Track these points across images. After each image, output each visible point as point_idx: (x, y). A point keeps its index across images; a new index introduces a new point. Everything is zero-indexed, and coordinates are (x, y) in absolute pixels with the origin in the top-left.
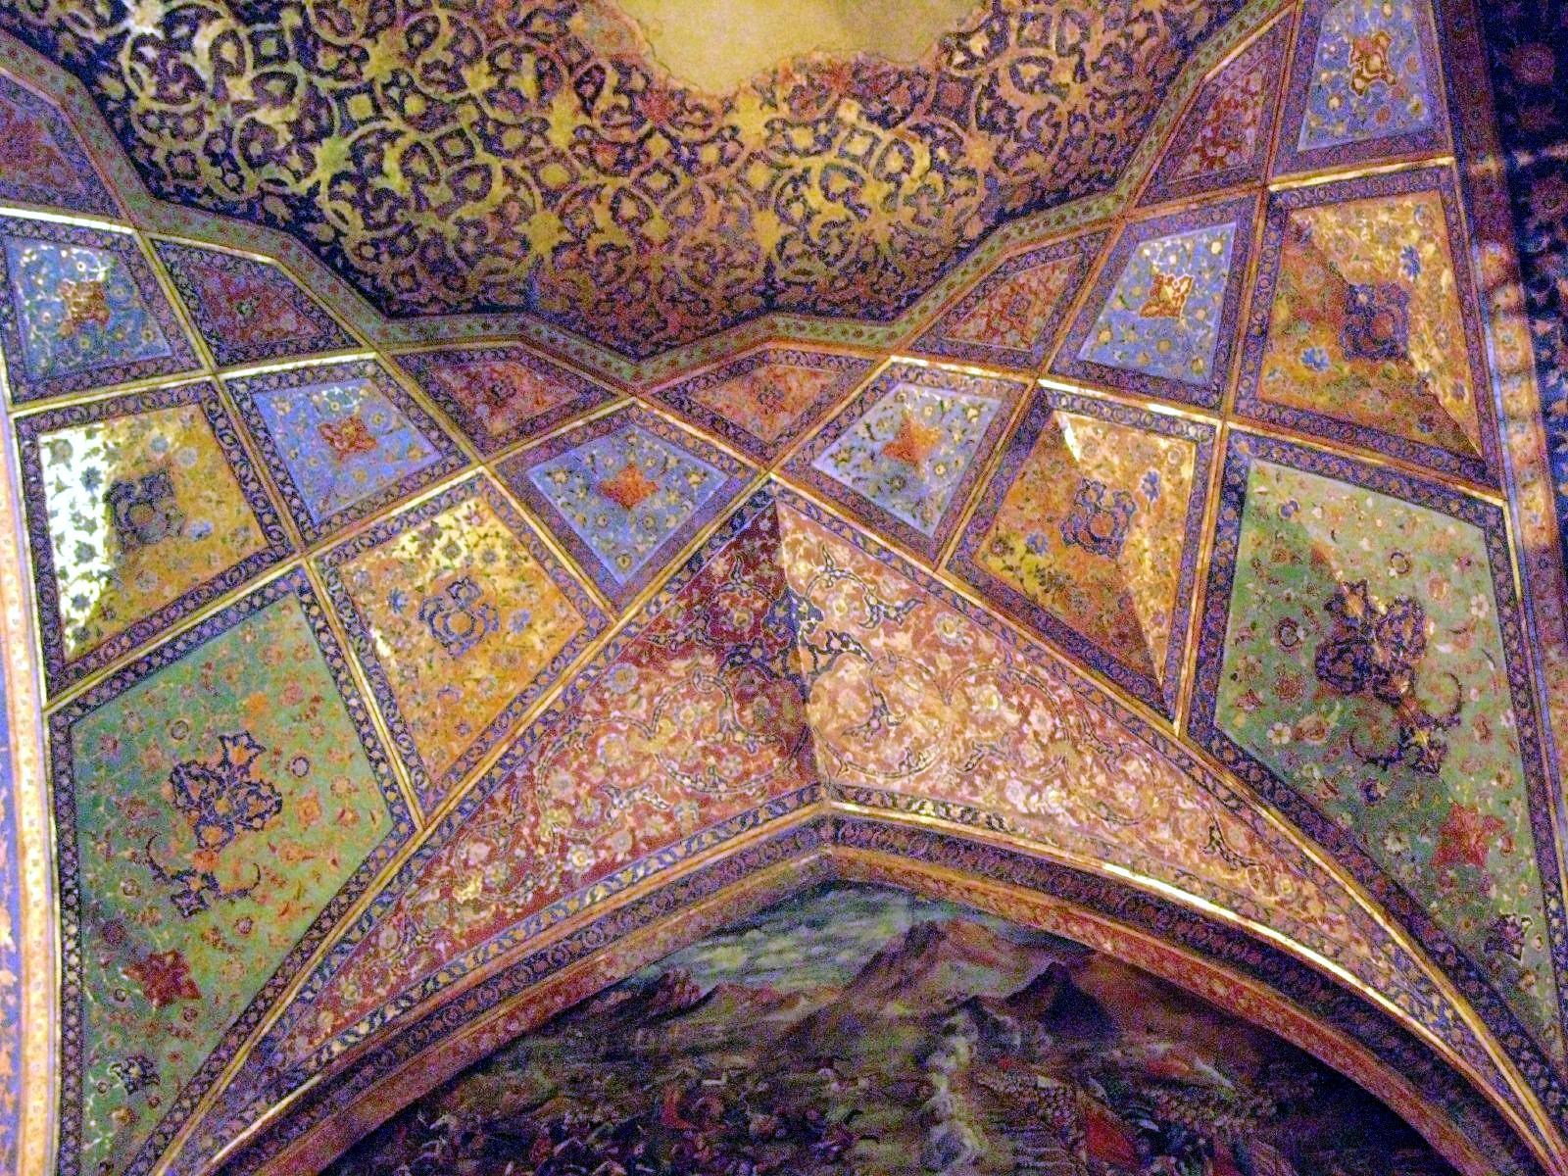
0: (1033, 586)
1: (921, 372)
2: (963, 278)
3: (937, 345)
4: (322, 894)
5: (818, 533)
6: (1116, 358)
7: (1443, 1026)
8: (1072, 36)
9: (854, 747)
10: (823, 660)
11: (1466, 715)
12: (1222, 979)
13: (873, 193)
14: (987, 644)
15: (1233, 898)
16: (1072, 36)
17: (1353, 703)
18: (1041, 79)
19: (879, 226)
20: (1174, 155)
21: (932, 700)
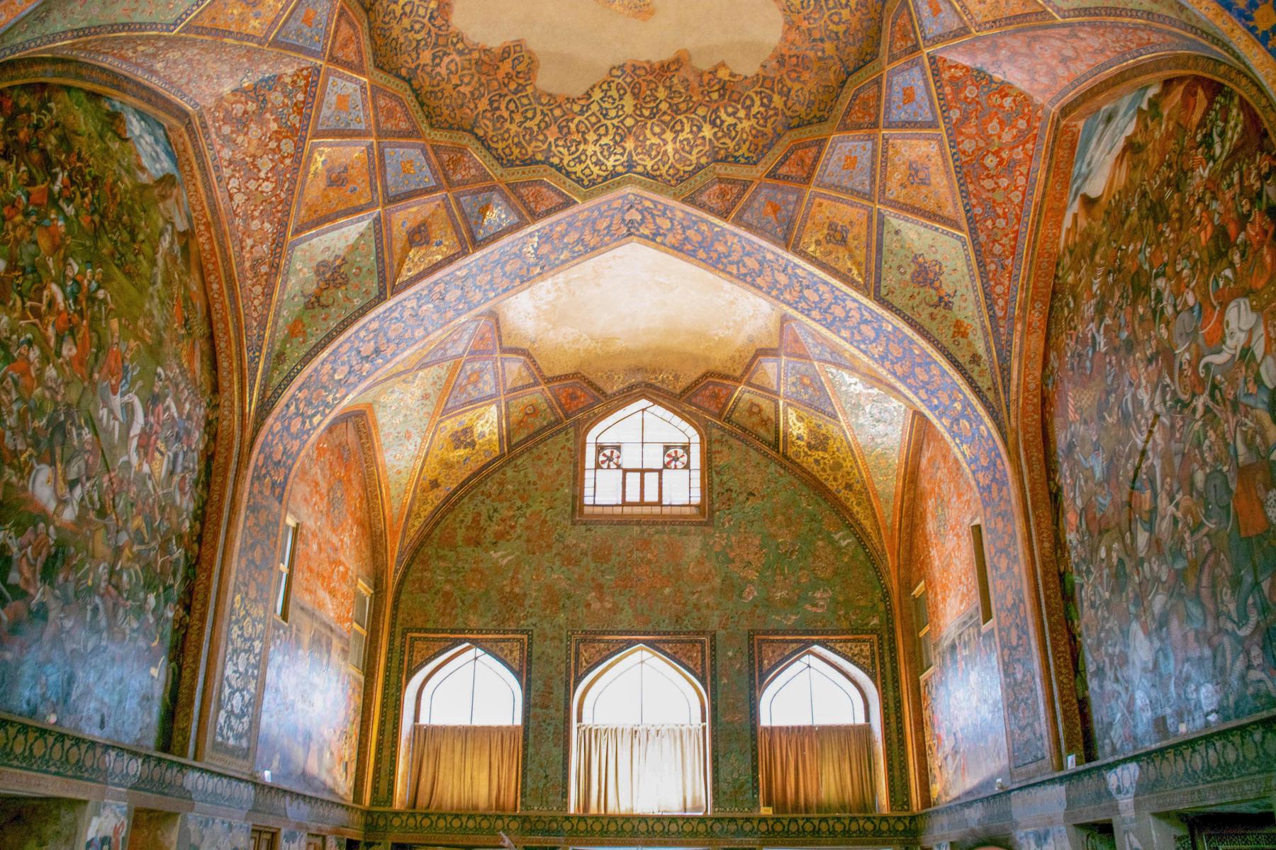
0: (312, 169)
1: (365, 93)
2: (394, 85)
3: (376, 90)
4: (138, 18)
5: (306, 86)
6: (387, 161)
7: (252, 360)
8: (466, 80)
9: (221, 115)
10: (252, 94)
11: (326, 310)
12: (221, 287)
13: (406, 22)
14: (288, 161)
15: (243, 271)
16: (466, 80)
17: (315, 278)
18: (451, 72)
19: (396, 31)
20: (446, 149)
21: (255, 142)
